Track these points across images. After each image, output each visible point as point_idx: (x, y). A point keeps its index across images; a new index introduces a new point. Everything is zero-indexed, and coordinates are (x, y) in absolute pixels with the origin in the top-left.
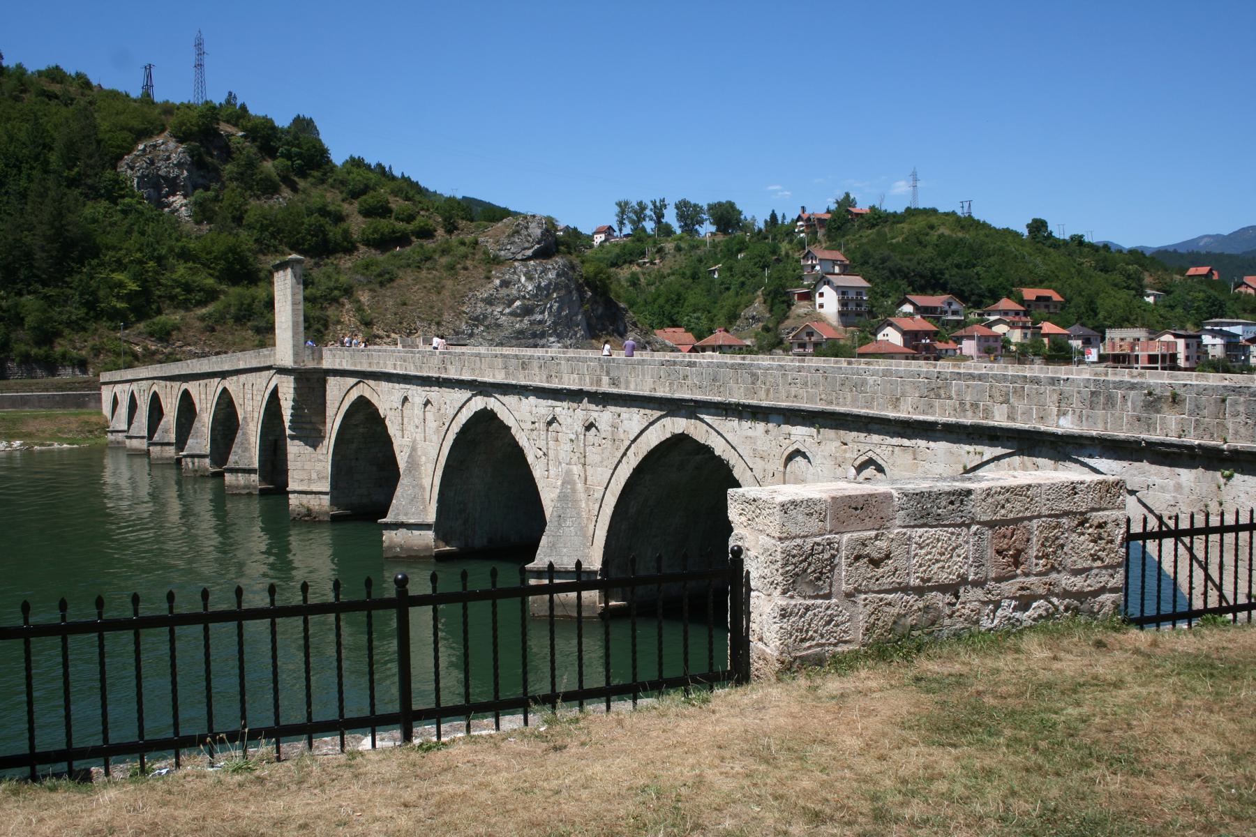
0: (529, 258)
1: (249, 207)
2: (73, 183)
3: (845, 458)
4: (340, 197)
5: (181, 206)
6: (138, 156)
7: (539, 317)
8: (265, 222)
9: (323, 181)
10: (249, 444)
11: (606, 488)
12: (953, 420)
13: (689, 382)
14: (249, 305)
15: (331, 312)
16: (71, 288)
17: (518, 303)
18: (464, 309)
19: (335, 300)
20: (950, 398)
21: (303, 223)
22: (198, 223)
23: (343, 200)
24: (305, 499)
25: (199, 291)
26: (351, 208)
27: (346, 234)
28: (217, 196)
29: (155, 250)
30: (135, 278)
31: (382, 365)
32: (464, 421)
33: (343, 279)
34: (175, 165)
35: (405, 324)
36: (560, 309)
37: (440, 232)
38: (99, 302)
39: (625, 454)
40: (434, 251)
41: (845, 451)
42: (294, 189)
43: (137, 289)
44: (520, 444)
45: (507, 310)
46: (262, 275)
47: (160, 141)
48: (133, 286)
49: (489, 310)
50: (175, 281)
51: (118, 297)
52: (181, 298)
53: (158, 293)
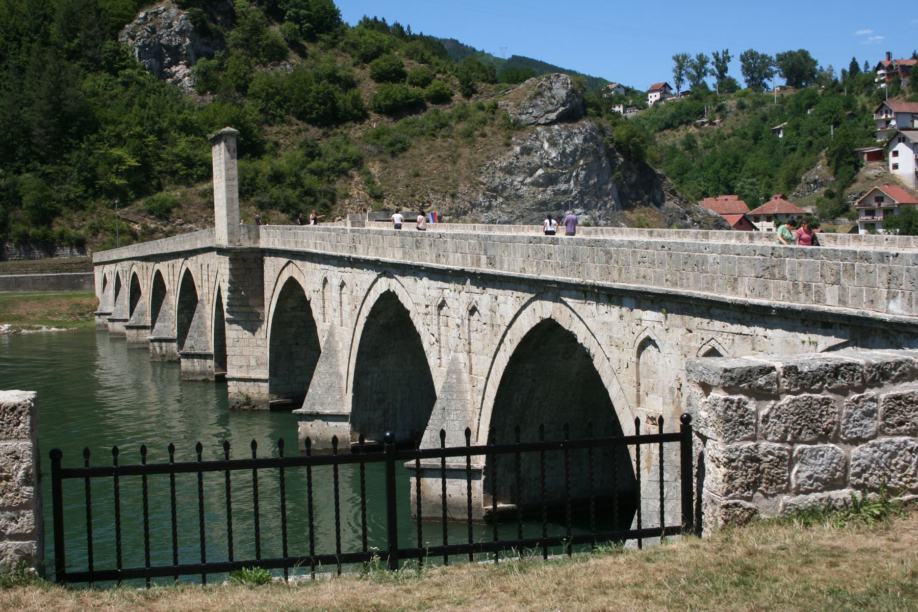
0: (553, 122)
1: (254, 75)
2: (73, 55)
3: (690, 348)
4: (352, 61)
5: (184, 76)
6: (140, 24)
7: (563, 187)
8: (271, 90)
9: (333, 45)
10: (205, 328)
11: (487, 379)
12: (785, 304)
13: (552, 261)
14: (253, 179)
15: (339, 185)
16: (70, 165)
17: (540, 172)
18: (481, 179)
19: (344, 172)
20: (784, 278)
21: (310, 91)
23: (355, 65)
24: (244, 387)
25: (201, 166)
26: (362, 74)
28: (222, 64)
29: (155, 123)
30: (135, 153)
31: (305, 244)
32: (372, 304)
33: (352, 149)
34: (177, 33)
35: (417, 197)
36: (588, 177)
37: (458, 96)
38: (98, 179)
39: (502, 341)
40: (451, 117)
41: (690, 340)
42: (303, 54)
43: (137, 164)
44: (417, 329)
45: (529, 180)
46: (267, 147)
47: (162, 8)
48: (133, 162)
49: (509, 180)
50: (176, 155)
51: (117, 174)
52: (181, 173)
53: (158, 168)
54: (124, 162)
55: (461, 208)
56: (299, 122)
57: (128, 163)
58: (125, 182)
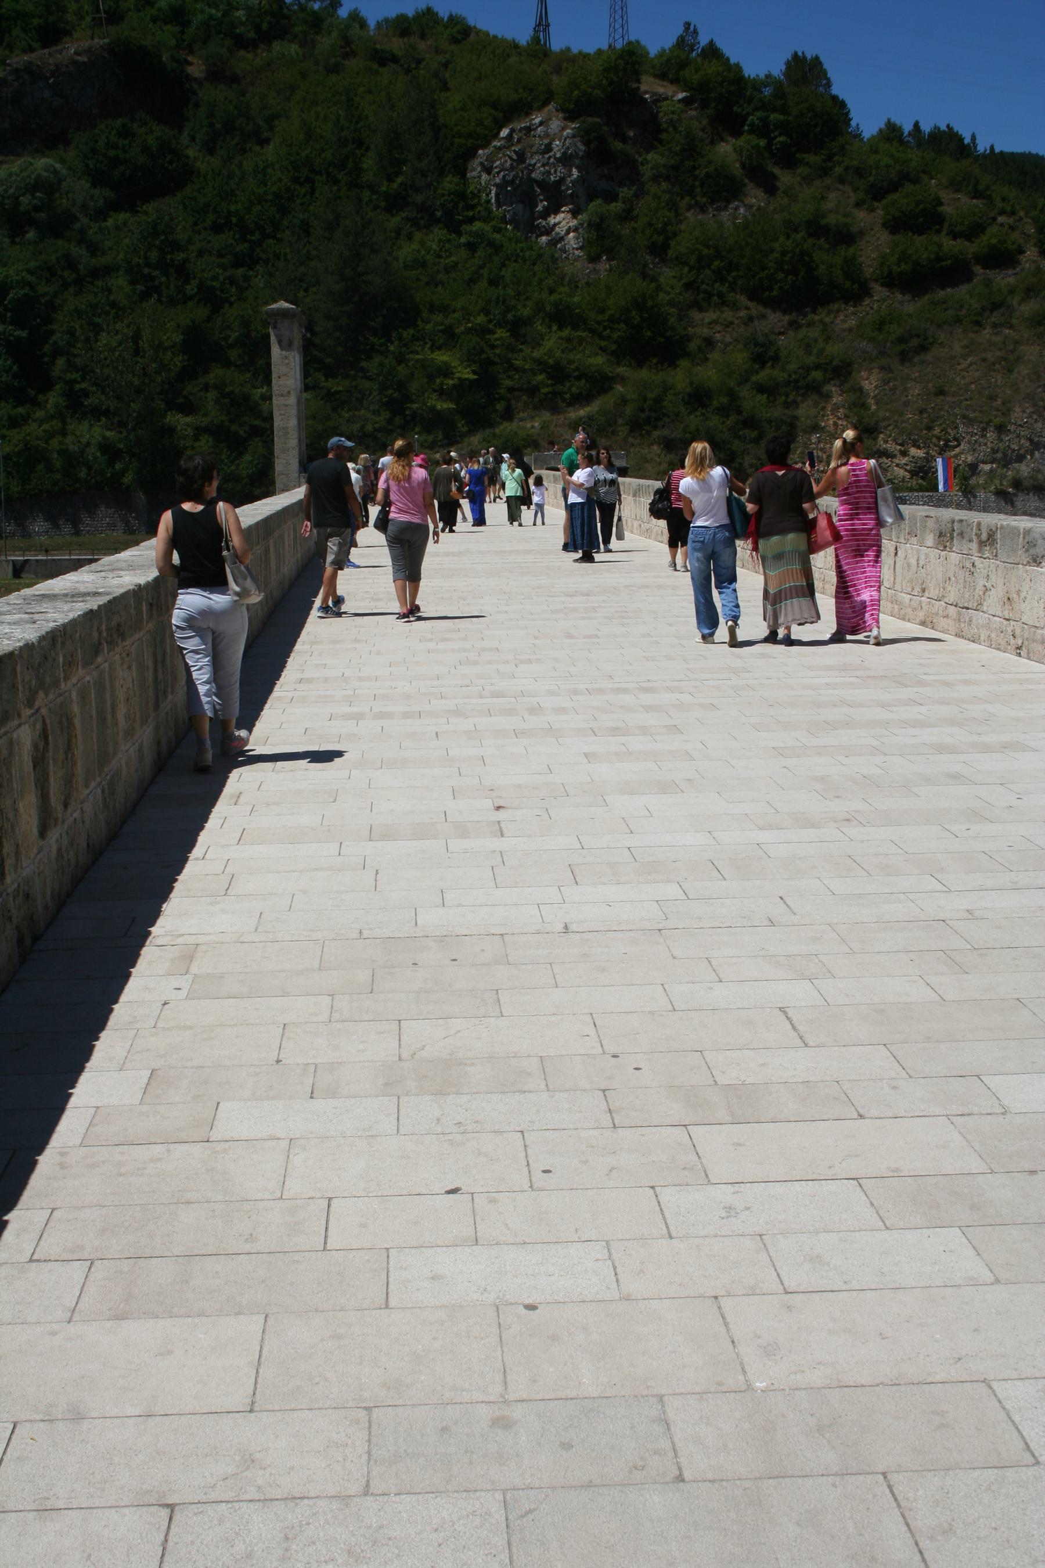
1: (683, 227)
2: (394, 203)
5: (568, 232)
6: (500, 148)
8: (705, 251)
9: (824, 172)
14: (658, 400)
15: (805, 411)
16: (369, 379)
19: (815, 388)
21: (772, 251)
22: (594, 259)
23: (858, 205)
25: (578, 378)
27: (851, 269)
28: (630, 210)
29: (509, 309)
33: (834, 349)
34: (559, 160)
35: (937, 431)
38: (412, 402)
40: (1012, 291)
42: (770, 188)
43: (472, 377)
46: (693, 346)
47: (537, 121)
48: (467, 374)
50: (538, 362)
51: (442, 393)
52: (544, 390)
53: (508, 383)
54: (453, 373)
55: (1014, 450)
56: (751, 304)
57: (457, 375)
58: (453, 406)
